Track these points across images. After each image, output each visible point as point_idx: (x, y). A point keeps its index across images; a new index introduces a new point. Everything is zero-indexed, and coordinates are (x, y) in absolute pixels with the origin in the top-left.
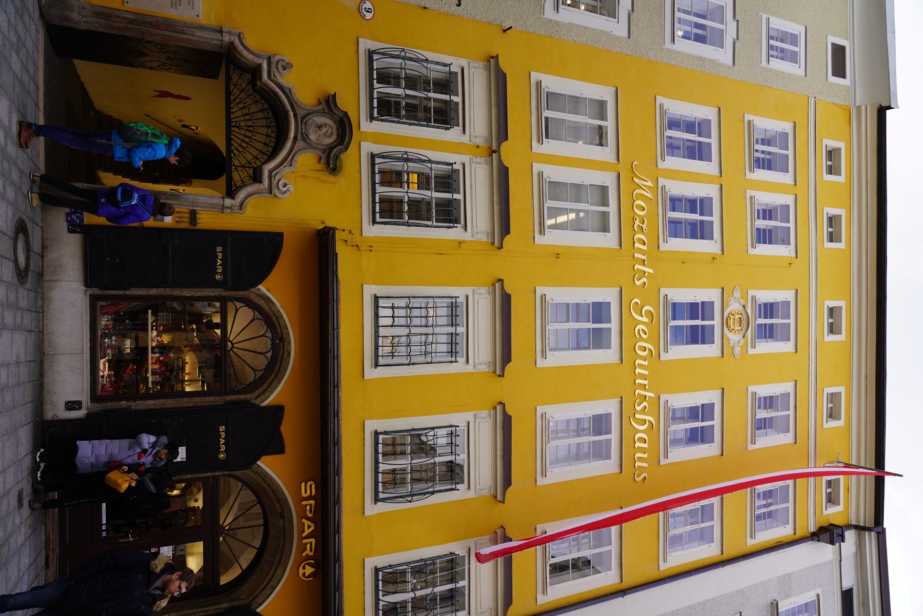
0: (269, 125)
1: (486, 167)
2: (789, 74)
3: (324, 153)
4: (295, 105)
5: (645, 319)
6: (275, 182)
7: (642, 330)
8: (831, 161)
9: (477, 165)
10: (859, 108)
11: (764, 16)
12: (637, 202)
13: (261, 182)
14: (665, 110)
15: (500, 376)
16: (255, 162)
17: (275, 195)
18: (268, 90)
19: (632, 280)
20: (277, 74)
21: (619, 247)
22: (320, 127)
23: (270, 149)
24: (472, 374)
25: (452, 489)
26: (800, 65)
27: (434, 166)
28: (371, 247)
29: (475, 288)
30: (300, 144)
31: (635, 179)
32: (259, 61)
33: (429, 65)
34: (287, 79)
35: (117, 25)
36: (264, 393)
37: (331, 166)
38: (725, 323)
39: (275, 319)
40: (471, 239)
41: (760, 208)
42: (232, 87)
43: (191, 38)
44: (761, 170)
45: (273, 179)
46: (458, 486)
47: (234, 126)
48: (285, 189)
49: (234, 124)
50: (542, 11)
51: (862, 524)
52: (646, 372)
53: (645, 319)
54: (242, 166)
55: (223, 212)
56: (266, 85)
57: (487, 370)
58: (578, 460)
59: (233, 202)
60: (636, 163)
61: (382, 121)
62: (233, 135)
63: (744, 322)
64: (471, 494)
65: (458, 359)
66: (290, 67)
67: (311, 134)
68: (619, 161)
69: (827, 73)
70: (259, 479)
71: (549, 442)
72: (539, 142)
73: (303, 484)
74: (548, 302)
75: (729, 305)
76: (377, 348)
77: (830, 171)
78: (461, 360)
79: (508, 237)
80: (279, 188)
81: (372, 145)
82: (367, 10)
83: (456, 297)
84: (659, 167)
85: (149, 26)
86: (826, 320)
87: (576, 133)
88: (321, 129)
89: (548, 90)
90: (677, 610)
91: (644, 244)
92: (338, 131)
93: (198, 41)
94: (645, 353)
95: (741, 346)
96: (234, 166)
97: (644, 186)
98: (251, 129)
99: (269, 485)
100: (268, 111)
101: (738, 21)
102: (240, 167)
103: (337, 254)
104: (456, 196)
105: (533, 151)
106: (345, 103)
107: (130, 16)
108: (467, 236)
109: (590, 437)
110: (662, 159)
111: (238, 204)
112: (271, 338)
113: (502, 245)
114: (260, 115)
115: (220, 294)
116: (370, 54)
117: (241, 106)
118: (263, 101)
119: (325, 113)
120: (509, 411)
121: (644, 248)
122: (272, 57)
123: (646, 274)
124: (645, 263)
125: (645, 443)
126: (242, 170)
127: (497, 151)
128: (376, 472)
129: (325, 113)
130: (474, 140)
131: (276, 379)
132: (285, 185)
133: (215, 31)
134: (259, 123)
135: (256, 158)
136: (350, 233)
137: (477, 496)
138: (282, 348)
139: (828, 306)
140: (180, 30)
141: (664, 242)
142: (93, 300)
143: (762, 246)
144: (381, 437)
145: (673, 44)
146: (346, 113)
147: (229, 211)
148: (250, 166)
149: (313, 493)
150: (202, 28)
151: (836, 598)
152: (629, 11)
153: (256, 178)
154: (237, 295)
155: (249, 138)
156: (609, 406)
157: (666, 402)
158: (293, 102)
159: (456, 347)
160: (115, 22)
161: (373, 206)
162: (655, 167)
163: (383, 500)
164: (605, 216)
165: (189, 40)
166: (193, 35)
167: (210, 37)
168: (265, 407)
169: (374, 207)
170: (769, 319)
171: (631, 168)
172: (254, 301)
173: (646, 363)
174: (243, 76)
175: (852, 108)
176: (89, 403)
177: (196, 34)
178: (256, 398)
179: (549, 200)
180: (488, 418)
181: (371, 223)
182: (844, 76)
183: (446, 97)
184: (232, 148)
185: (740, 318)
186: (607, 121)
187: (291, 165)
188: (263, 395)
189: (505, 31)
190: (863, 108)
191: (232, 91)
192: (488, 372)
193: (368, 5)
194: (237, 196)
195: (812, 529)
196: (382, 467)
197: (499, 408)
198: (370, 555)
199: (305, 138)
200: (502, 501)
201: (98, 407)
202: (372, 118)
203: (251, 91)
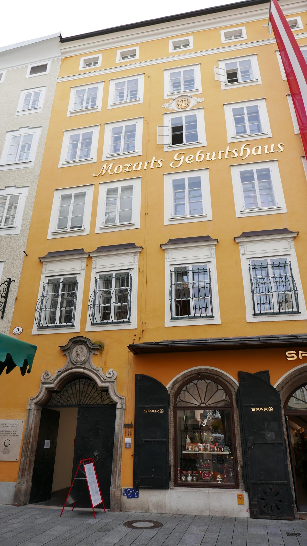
0: (88, 384)
1: (98, 260)
3: (92, 352)
4: (66, 369)
5: (182, 158)
6: (108, 380)
7: (189, 159)
8: (91, 64)
9: (97, 265)
10: (62, 53)
12: (115, 171)
13: (108, 387)
14: (66, 162)
15: (218, 242)
16: (99, 391)
17: (115, 379)
18: (59, 384)
19: (159, 168)
20: (51, 379)
21: (141, 179)
22: (78, 355)
23: (92, 382)
24: (217, 259)
25: (290, 265)
26: (41, 90)
27: (97, 290)
28: (143, 323)
29: (166, 261)
30: (87, 366)
31: (103, 174)
32: (44, 389)
35: (28, 465)
36: (231, 384)
37: (98, 348)
38: (183, 110)
39: (186, 378)
40: (138, 265)
41: (119, 100)
42: (59, 404)
43: (33, 426)
44: (96, 103)
45: (106, 380)
46: (288, 262)
47: (80, 403)
48: (111, 373)
49: (79, 403)
52: (214, 153)
53: (183, 157)
54: (101, 398)
55: (125, 409)
56: (56, 385)
57: (214, 250)
58: (271, 188)
59: (119, 403)
61: (74, 320)
63: (183, 98)
64: (293, 253)
65: (208, 268)
66: (47, 372)
67: (81, 359)
68: (93, 184)
69: (45, 75)
70: (286, 386)
71: (259, 208)
73: (288, 359)
74: (173, 217)
75: (173, 109)
76: (202, 317)
77: (96, 63)
78: (209, 265)
79: (137, 244)
80: (111, 377)
82: (18, 331)
83: (171, 272)
84: (96, 161)
85: (27, 448)
86: (182, 49)
88: (78, 354)
89: (56, 228)
91: (139, 164)
92: (80, 345)
93: (35, 422)
94: (203, 155)
95: (197, 98)
96: (101, 403)
97: (106, 168)
98: (81, 393)
99: (290, 380)
100: (71, 384)
101: (19, 128)
102: (101, 399)
103: (144, 343)
104: (114, 276)
105: (89, 234)
106: (64, 342)
107: (23, 458)
108: (136, 268)
109: (255, 183)
110: (92, 160)
111: (120, 400)
112: (198, 380)
113: (140, 247)
115: (172, 410)
116: (40, 328)
117: (69, 399)
118: (66, 387)
119: (70, 352)
120: (239, 234)
121: (141, 164)
122: (42, 382)
123: (156, 161)
124: (149, 162)
125: (258, 148)
126: (103, 398)
127: (89, 254)
128: (280, 313)
129: (70, 352)
130: (84, 268)
131: (222, 377)
133: (29, 412)
135: (96, 390)
136: (135, 335)
137: (295, 250)
138: (203, 374)
139: (173, 50)
140: (29, 432)
141: (137, 153)
142: (177, 485)
143: (138, 96)
144: (257, 312)
145: (31, 162)
146: (69, 340)
147: (124, 405)
148: (101, 393)
149: (294, 352)
150: (28, 420)
152: (15, 188)
154: (173, 401)
155: (86, 394)
156: (236, 173)
157: (232, 138)
158: (65, 370)
159: (200, 270)
160: (26, 466)
161: (120, 323)
162: (96, 163)
163: (297, 306)
165: (34, 427)
166: (32, 425)
167: (33, 415)
168: (239, 384)
169: (121, 322)
170: (181, 84)
171: (97, 177)
172: (176, 390)
173: (208, 154)
175: (63, 57)
176: (239, 490)
177: (31, 423)
178: (234, 388)
179: (115, 222)
180: (244, 247)
181: (130, 324)
182: (46, 66)
183: (61, 285)
184: (91, 404)
185: (181, 101)
186: (72, 194)
187: (99, 370)
188: (232, 385)
189: (27, 255)
190: (62, 51)
191: (61, 404)
192: (216, 249)
193: (15, 330)
194: (115, 401)
196: (276, 310)
197: (237, 241)
199: (84, 363)
200: (297, 233)
201: (241, 485)
202: (73, 326)
203: (61, 393)
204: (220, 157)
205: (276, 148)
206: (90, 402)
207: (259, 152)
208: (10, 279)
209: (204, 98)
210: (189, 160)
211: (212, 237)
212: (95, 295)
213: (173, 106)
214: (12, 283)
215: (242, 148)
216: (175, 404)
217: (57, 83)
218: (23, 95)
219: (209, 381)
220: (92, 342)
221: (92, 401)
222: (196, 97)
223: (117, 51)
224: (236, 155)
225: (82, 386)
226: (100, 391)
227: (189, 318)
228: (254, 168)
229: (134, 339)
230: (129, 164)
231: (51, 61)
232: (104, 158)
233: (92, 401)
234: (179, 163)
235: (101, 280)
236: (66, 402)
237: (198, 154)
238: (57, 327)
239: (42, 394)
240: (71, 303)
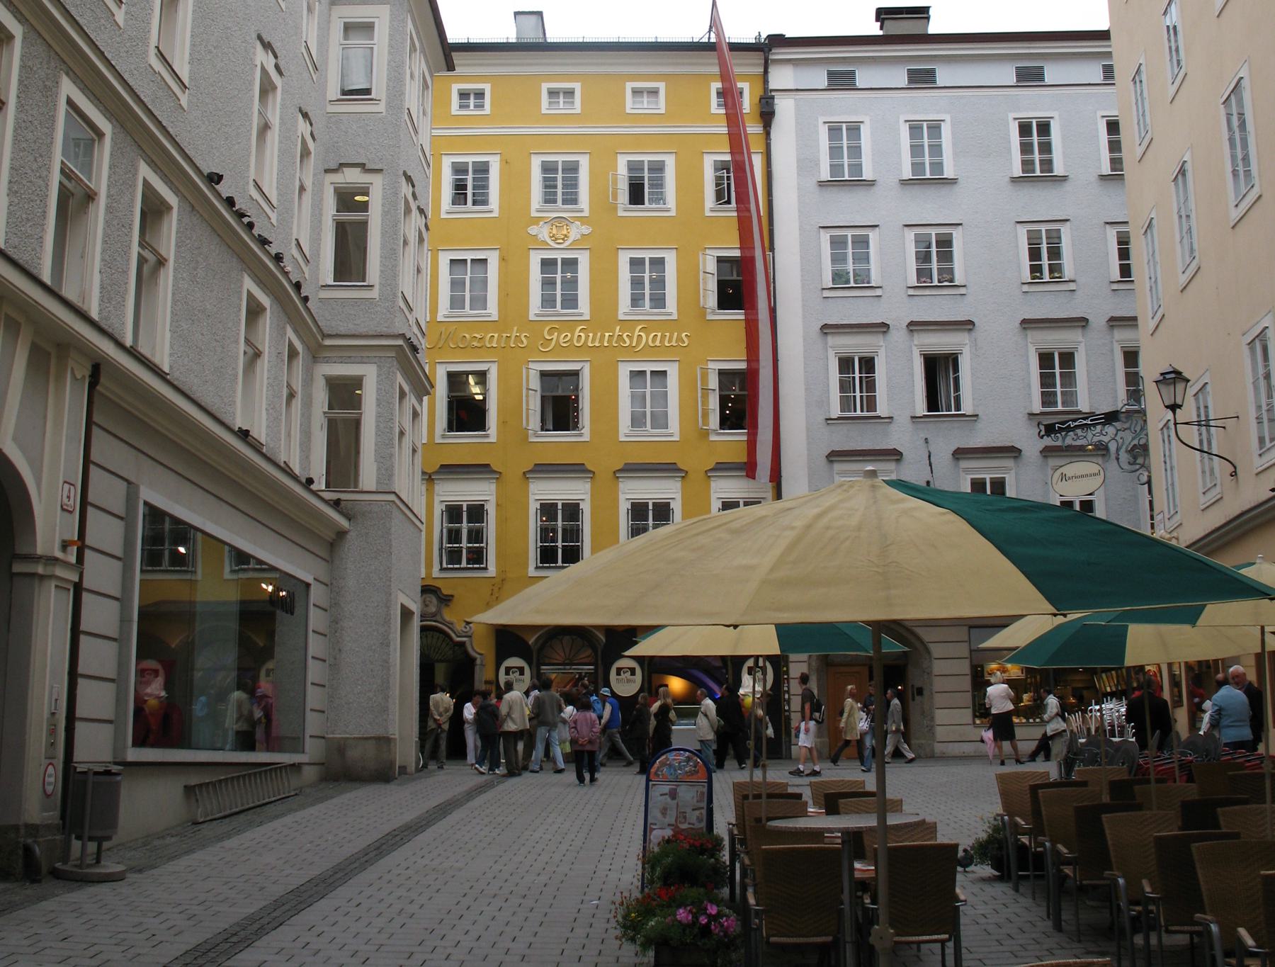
6: (464, 634)
24: (592, 495)
30: (438, 618)
53: (556, 334)
64: (678, 496)
90: (803, 300)
153: (462, 644)
156: (624, 371)
187: (452, 624)
199: (434, 615)
204: (606, 344)
205: (680, 339)
207: (658, 343)
213: (543, 232)
215: (637, 333)
216: (538, 660)
219: (574, 637)
230: (478, 333)
234: (551, 343)
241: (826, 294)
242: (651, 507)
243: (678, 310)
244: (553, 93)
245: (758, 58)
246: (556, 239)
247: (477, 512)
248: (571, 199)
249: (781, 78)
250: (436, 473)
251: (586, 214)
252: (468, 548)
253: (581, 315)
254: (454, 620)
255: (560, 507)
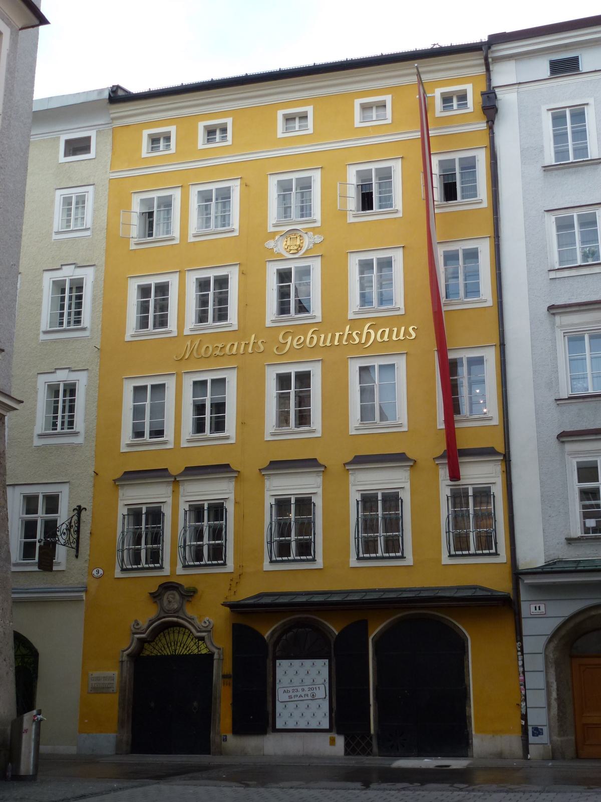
1: (186, 484)
2: (95, 203)
6: (204, 629)
7: (297, 341)
11: (55, 237)
20: (142, 629)
22: (170, 602)
23: (187, 631)
27: (187, 524)
31: (187, 357)
33: (125, 530)
34: (143, 623)
37: (192, 594)
48: (207, 622)
49: (174, 653)
50: (80, 445)
51: (483, 61)
53: (290, 338)
54: (198, 648)
55: (223, 660)
56: (148, 635)
57: (322, 477)
60: (175, 357)
61: (162, 560)
62: (181, 652)
64: (407, 486)
72: (166, 443)
79: (232, 466)
81: (178, 567)
87: (158, 411)
95: (314, 235)
97: (191, 347)
101: (62, 265)
108: (232, 496)
111: (217, 651)
114: (167, 637)
116: (123, 570)
117: (163, 649)
120: (350, 459)
127: (175, 477)
132: (205, 622)
134: (172, 638)
144: (361, 555)
146: (160, 586)
147: (222, 656)
151: (555, 84)
156: (354, 368)
164: (214, 381)
173: (323, 336)
174: (146, 648)
181: (225, 566)
187: (193, 619)
189: (97, 474)
190: (112, 116)
195: (483, 126)
198: (440, 560)
199: (176, 611)
202: (161, 568)
203: (154, 643)
205: (406, 333)
206: (186, 652)
207: (386, 338)
208: (79, 507)
209: (322, 237)
210: (298, 343)
211: (321, 461)
212: (185, 531)
213: (280, 246)
214: (83, 512)
217: (110, 179)
218: (59, 195)
220: (185, 587)
221: (189, 650)
222: (311, 231)
223: (199, 123)
224: (357, 340)
225: (176, 635)
226: (197, 640)
227: (289, 561)
228: (376, 363)
229: (230, 584)
231: (95, 131)
232: (187, 332)
233: (189, 650)
234: (286, 347)
235: (191, 512)
236: (160, 653)
237: (309, 335)
238: (143, 569)
239: (134, 645)
240: (156, 538)
241: (553, 275)
242: (380, 498)
243: (405, 305)
244: (289, 119)
245: (476, 59)
246: (291, 250)
247: (218, 510)
248: (305, 210)
249: (503, 75)
250: (181, 475)
251: (318, 224)
252: (209, 545)
253: (314, 317)
254: (195, 616)
255: (293, 501)
